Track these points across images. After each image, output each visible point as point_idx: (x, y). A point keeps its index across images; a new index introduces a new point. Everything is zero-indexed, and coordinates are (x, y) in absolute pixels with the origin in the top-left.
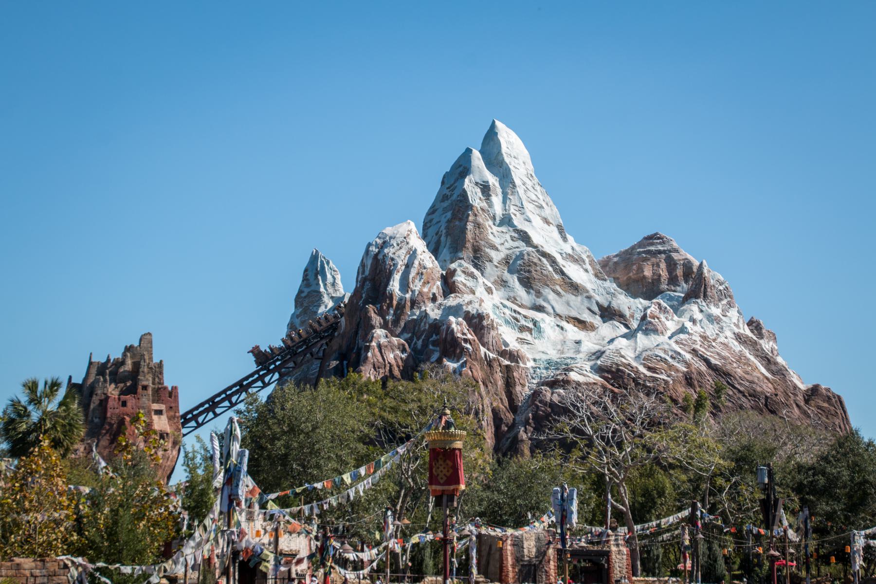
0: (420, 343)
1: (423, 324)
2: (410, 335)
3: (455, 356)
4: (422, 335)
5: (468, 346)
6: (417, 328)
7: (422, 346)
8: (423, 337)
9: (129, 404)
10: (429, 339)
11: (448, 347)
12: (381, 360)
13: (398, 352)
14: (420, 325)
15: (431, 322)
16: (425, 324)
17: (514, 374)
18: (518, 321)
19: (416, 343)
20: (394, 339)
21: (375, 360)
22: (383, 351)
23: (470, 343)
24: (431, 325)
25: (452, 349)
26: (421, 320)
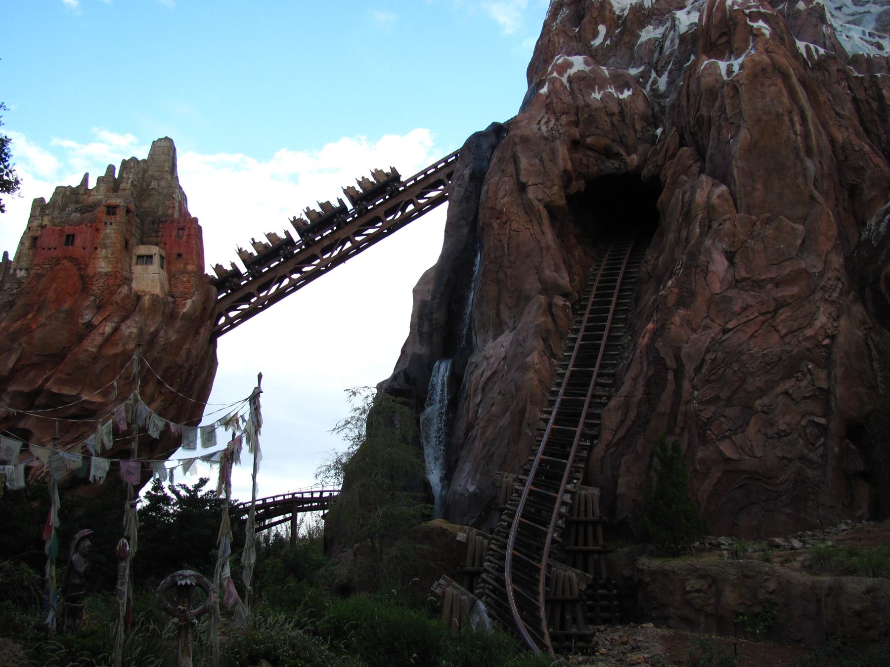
0: (662, 83)
1: (668, 43)
2: (642, 69)
3: (731, 52)
4: (664, 67)
5: (761, 23)
6: (656, 55)
7: (670, 83)
8: (670, 67)
9: (78, 241)
10: (681, 66)
11: (714, 35)
12: (568, 99)
13: (611, 90)
14: (662, 48)
15: (683, 28)
16: (672, 41)
17: (884, 92)
18: (880, 47)
19: (655, 82)
20: (603, 68)
21: (555, 101)
22: (575, 86)
23: (766, 21)
24: (683, 38)
25: (724, 40)
26: (664, 36)
